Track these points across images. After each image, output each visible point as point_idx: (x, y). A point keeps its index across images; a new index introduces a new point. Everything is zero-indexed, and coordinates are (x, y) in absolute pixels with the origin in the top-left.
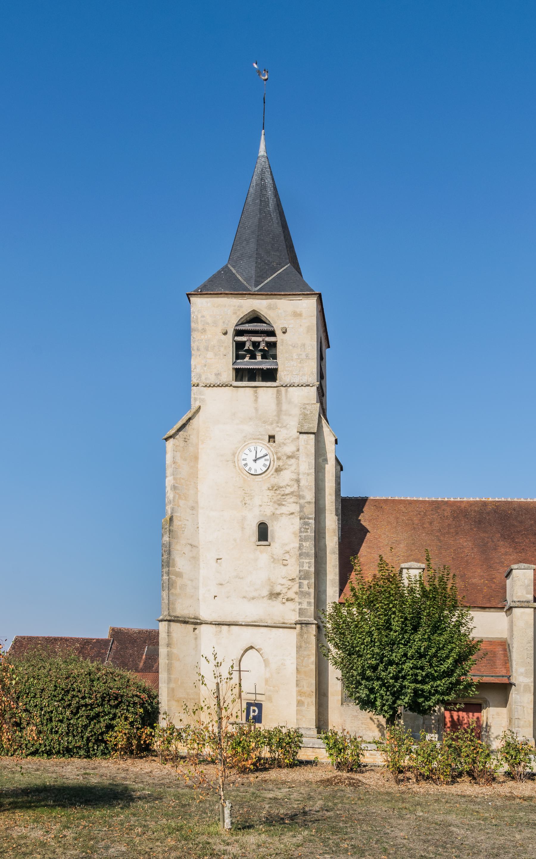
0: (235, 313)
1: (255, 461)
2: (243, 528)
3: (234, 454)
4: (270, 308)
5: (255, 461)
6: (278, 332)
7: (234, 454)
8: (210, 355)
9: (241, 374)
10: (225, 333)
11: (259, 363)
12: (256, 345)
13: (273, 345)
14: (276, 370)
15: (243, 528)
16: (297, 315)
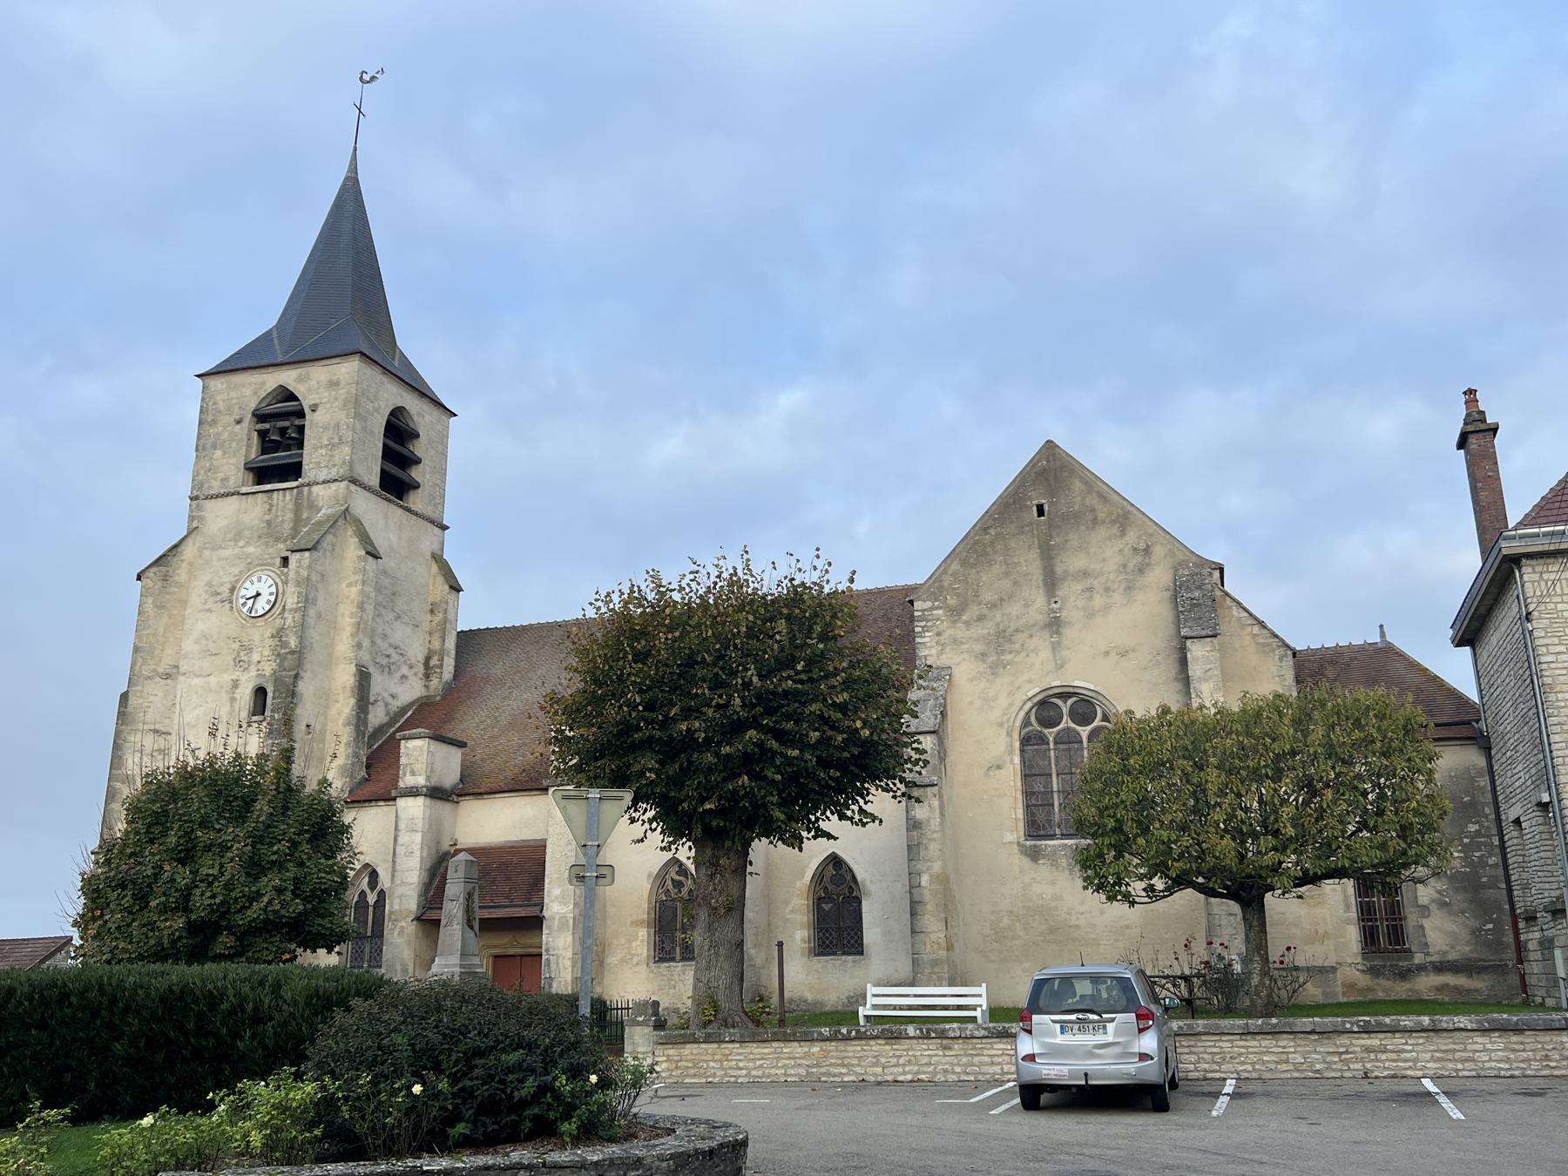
0: (255, 393)
1: (258, 594)
2: (233, 700)
3: (232, 590)
4: (300, 380)
5: (258, 594)
6: (307, 411)
7: (232, 590)
8: (218, 453)
9: (262, 474)
10: (239, 422)
11: (282, 457)
12: (283, 431)
13: (301, 429)
14: (300, 464)
15: (233, 700)
16: (333, 384)
